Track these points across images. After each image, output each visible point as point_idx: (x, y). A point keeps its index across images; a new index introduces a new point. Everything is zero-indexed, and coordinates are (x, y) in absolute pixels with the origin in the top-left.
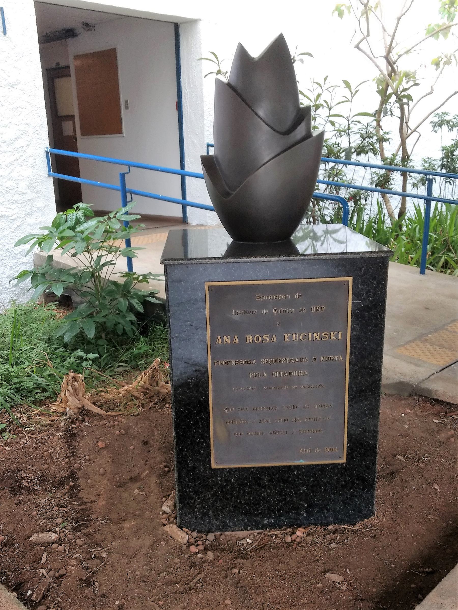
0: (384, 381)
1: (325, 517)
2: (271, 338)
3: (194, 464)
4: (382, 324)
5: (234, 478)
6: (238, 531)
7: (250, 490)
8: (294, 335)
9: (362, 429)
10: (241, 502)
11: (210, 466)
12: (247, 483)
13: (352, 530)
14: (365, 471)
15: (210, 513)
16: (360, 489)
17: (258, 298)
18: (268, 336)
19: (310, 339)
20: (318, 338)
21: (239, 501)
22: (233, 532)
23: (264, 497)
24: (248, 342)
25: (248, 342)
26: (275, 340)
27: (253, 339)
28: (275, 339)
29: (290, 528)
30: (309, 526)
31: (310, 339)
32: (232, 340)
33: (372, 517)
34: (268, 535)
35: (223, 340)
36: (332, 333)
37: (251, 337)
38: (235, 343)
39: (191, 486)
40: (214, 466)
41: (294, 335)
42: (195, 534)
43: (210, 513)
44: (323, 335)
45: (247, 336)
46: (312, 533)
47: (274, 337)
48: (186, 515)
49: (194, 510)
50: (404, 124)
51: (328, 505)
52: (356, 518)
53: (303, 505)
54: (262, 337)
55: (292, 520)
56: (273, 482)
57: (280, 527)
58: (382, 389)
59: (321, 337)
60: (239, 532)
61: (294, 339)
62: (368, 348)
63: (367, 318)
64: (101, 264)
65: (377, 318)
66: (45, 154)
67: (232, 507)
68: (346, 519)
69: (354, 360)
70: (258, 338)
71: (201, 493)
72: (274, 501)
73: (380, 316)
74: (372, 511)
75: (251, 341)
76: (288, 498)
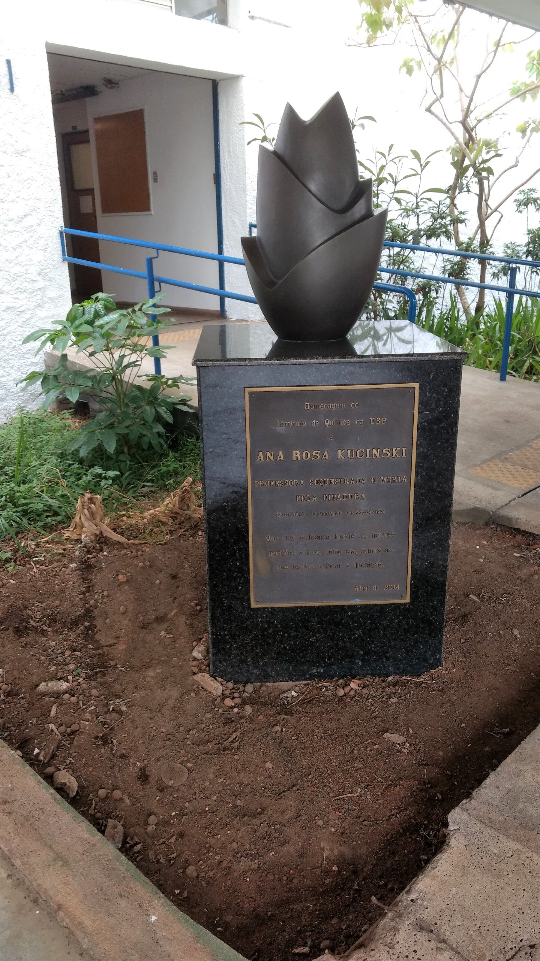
0: (455, 507)
1: (384, 666)
2: (322, 454)
3: (230, 603)
4: (454, 439)
6: (281, 681)
7: (295, 633)
8: (349, 451)
9: (429, 563)
10: (285, 647)
11: (249, 604)
12: (292, 626)
13: (416, 683)
14: (431, 613)
15: (249, 660)
16: (426, 634)
17: (307, 407)
18: (319, 452)
20: (378, 456)
21: (282, 646)
23: (312, 642)
24: (295, 459)
25: (295, 459)
26: (327, 457)
28: (327, 455)
29: (342, 678)
30: (365, 676)
31: (368, 456)
32: (276, 456)
33: (440, 668)
34: (317, 687)
35: (265, 456)
36: (394, 449)
37: (299, 453)
39: (227, 628)
40: (253, 605)
41: (349, 451)
42: (230, 685)
43: (249, 660)
44: (384, 451)
45: (294, 452)
46: (368, 685)
47: (326, 453)
48: (220, 662)
49: (229, 657)
50: (484, 203)
51: (388, 652)
52: (421, 668)
53: (358, 653)
54: (311, 453)
55: (344, 670)
57: (331, 678)
58: (454, 517)
59: (382, 454)
61: (349, 457)
62: (437, 467)
66: (59, 234)
68: (409, 669)
69: (420, 481)
70: (307, 454)
71: (239, 636)
72: (324, 647)
73: (452, 430)
74: (439, 660)
75: (299, 458)
76: (341, 644)
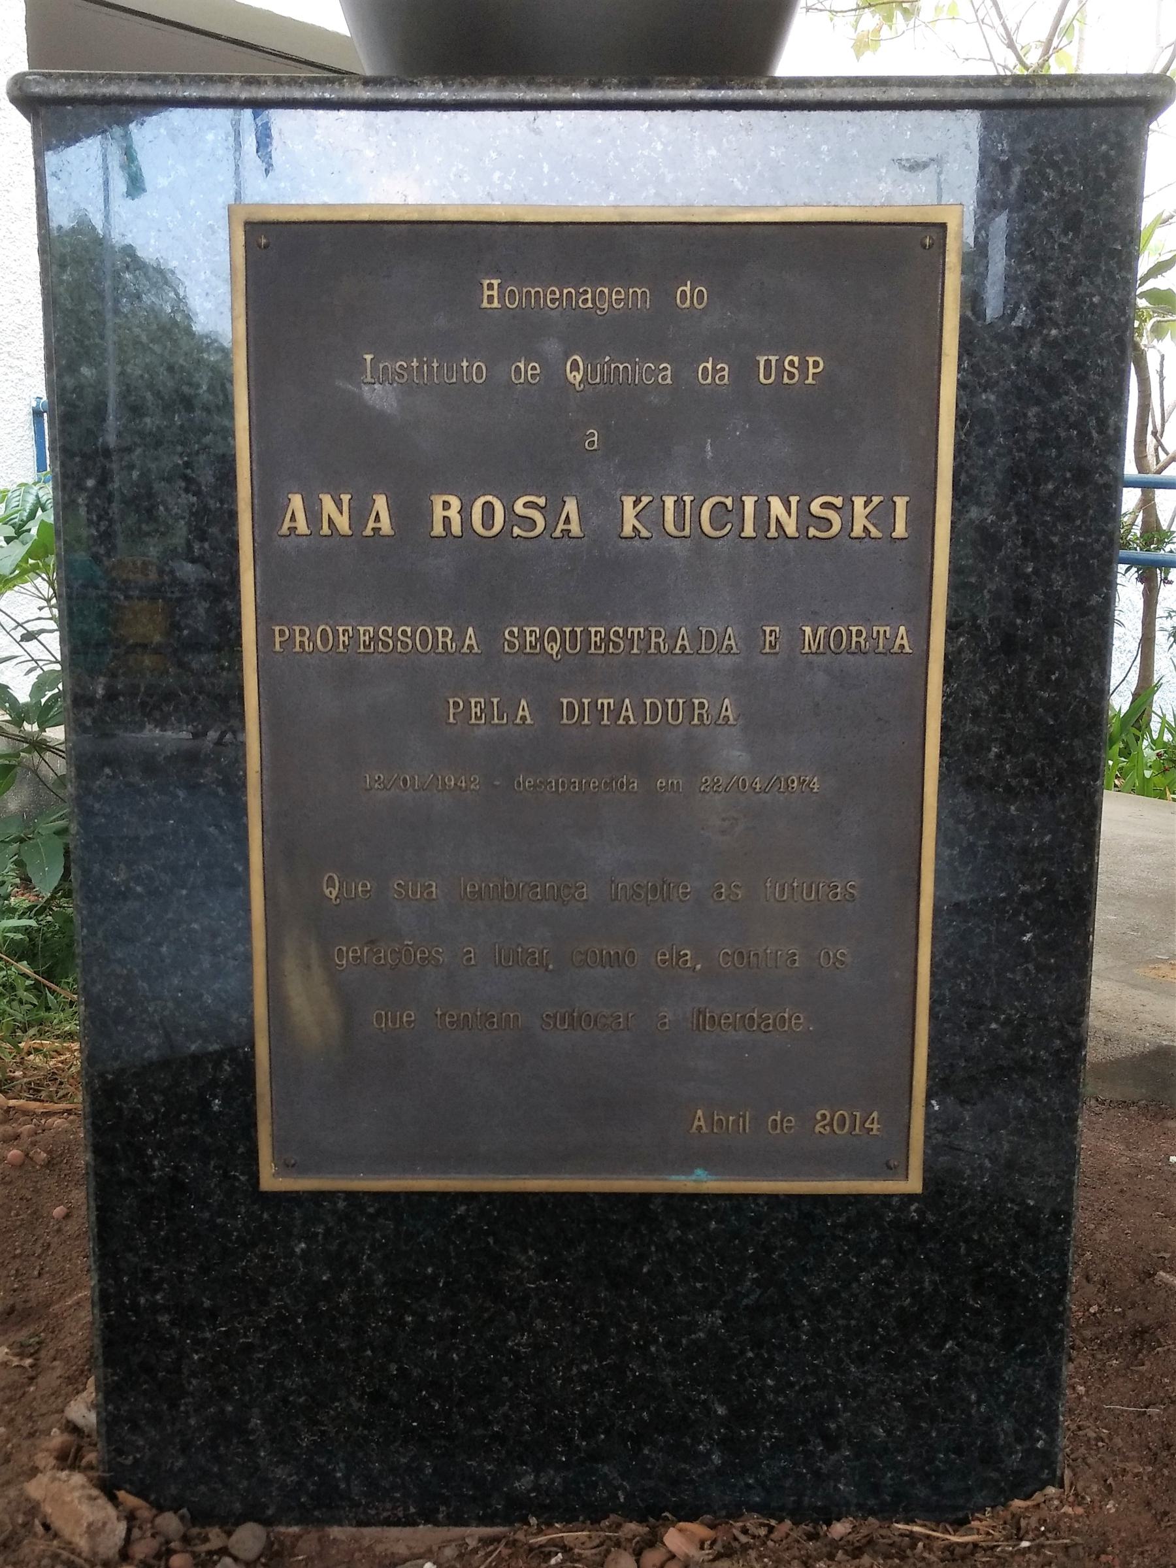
0: (1095, 1052)
1: (817, 1474)
2: (553, 511)
3: (177, 1168)
4: (1109, 472)
5: (372, 1247)
6: (388, 1523)
7: (448, 1313)
8: (670, 502)
9: (1003, 1024)
10: (403, 1373)
11: (255, 1177)
12: (435, 1278)
13: (950, 1548)
14: (1014, 1246)
15: (256, 1421)
16: (988, 1338)
17: (491, 298)
18: (541, 501)
19: (749, 531)
20: (791, 529)
21: (393, 1369)
22: (367, 1531)
23: (516, 1353)
24: (438, 529)
25: (438, 529)
26: (575, 528)
27: (465, 512)
28: (574, 517)
29: (642, 1520)
30: (734, 1513)
31: (749, 531)
32: (360, 514)
33: (1051, 1490)
34: (531, 1549)
35: (313, 514)
36: (859, 502)
37: (455, 503)
38: (376, 530)
39: (162, 1280)
40: (270, 1179)
41: (670, 502)
42: (170, 1523)
43: (256, 1421)
44: (815, 507)
45: (438, 501)
46: (745, 1548)
47: (571, 507)
48: (135, 1427)
49: (173, 1405)
50: (1150, 440)
51: (832, 1414)
52: (968, 1490)
53: (706, 1407)
54: (509, 510)
55: (649, 1484)
56: (562, 1279)
57: (595, 1515)
58: (1090, 1086)
59: (806, 517)
60: (394, 1532)
61: (670, 527)
62: (1038, 594)
63: (1032, 436)
64: (24, 528)
65: (1085, 436)
66: (31, 417)
67: (360, 1399)
68: (922, 1492)
69: (967, 656)
70: (488, 508)
71: (212, 1314)
72: (567, 1380)
73: (1102, 424)
74: (1047, 1458)
75: (456, 529)
76: (635, 1368)
